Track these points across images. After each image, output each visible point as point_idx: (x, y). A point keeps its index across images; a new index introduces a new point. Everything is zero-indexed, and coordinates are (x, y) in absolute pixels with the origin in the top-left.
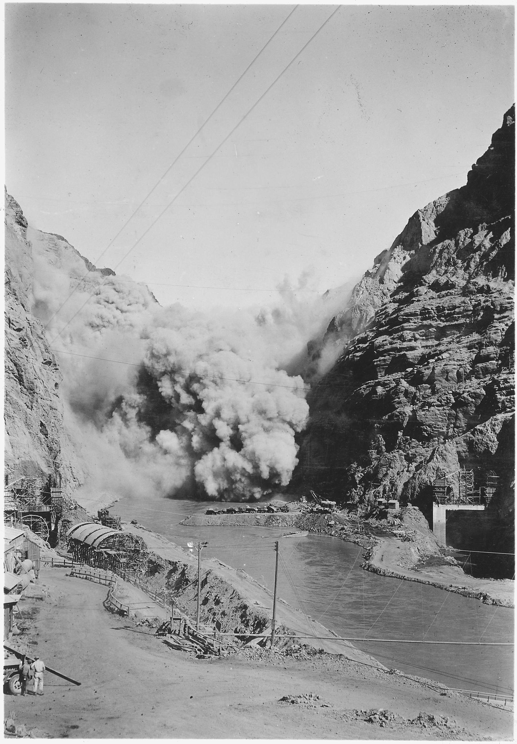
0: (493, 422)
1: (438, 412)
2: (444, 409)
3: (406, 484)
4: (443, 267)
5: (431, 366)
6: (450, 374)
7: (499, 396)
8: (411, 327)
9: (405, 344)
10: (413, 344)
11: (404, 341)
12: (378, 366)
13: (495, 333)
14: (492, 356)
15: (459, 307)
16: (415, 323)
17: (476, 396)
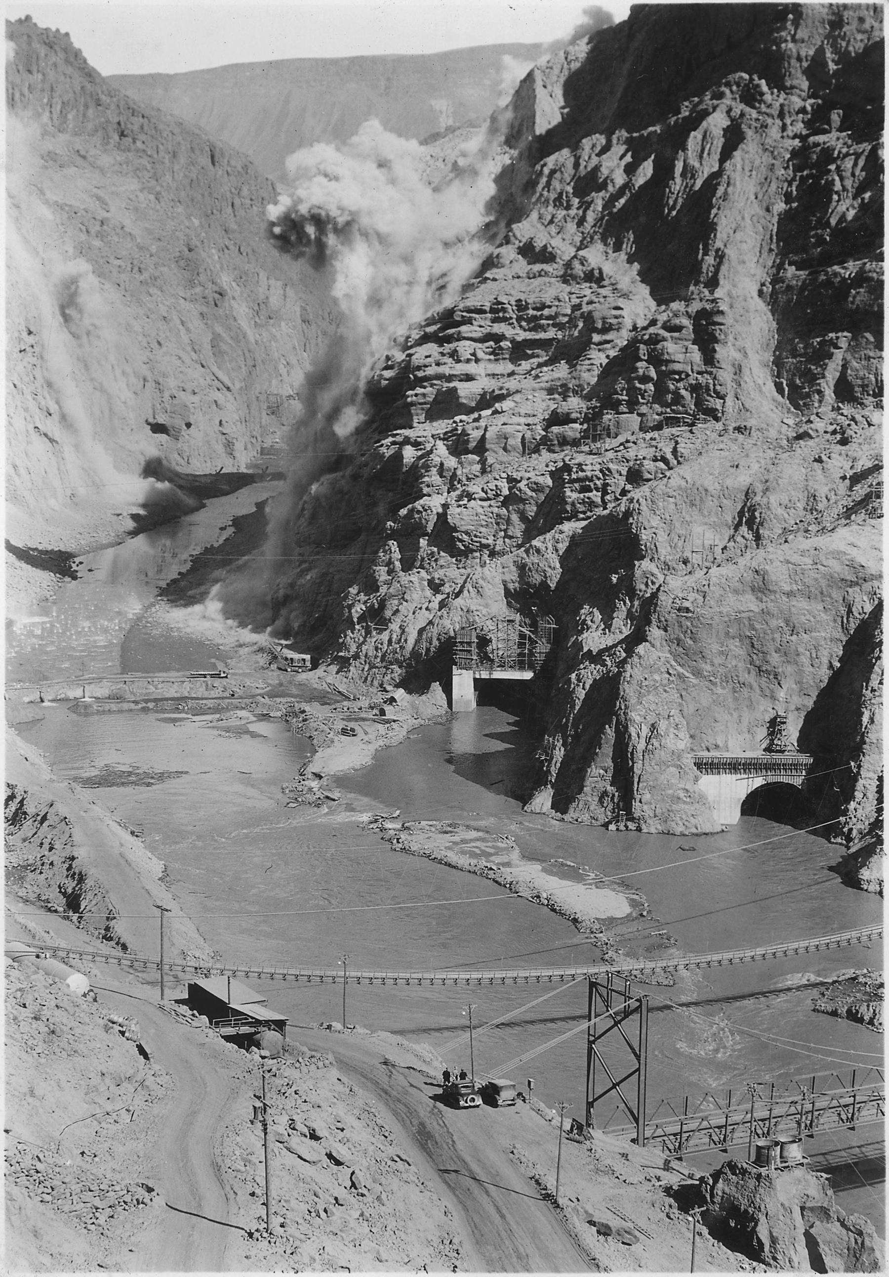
0: (557, 536)
1: (481, 511)
2: (490, 506)
3: (421, 631)
4: (550, 208)
5: (482, 423)
6: (511, 442)
7: (568, 493)
8: (474, 335)
9: (460, 369)
10: (471, 368)
11: (458, 361)
12: (413, 404)
13: (589, 370)
14: (574, 416)
15: (550, 307)
16: (481, 326)
17: (537, 488)
